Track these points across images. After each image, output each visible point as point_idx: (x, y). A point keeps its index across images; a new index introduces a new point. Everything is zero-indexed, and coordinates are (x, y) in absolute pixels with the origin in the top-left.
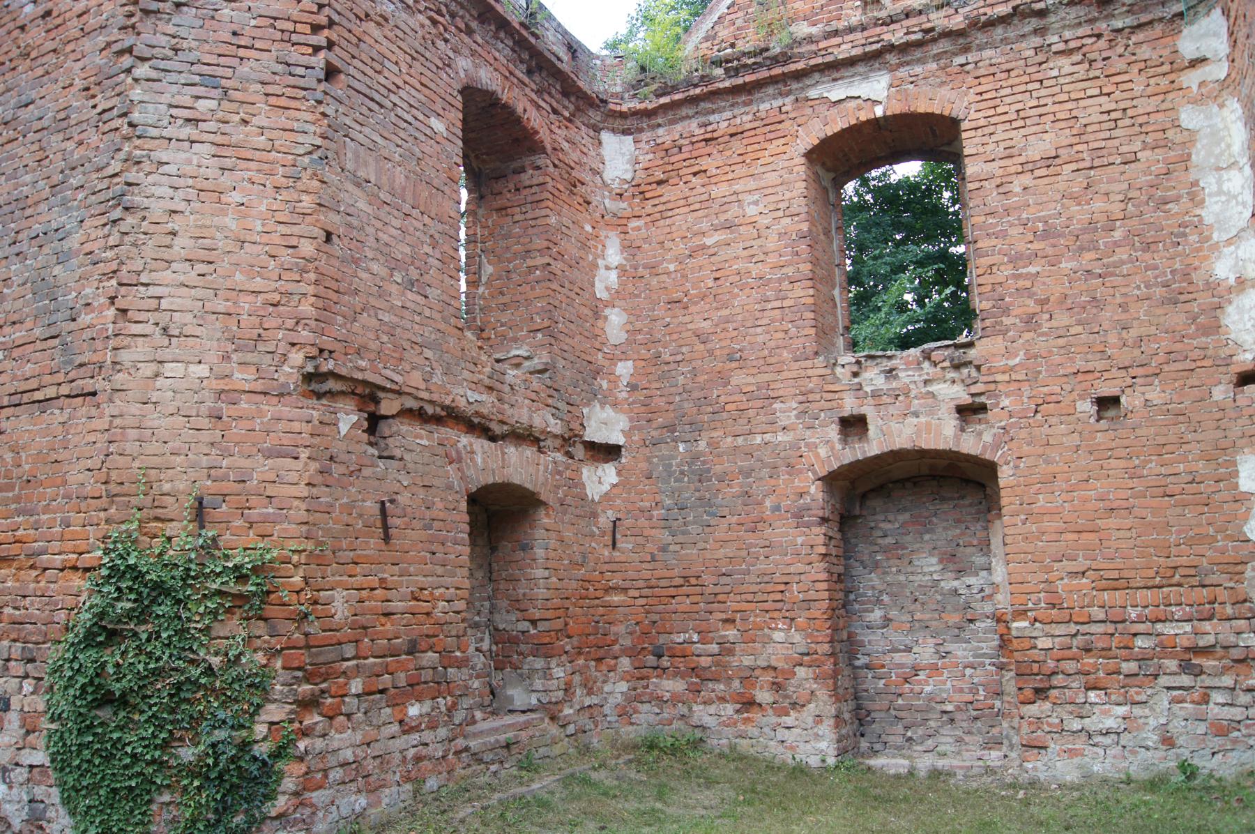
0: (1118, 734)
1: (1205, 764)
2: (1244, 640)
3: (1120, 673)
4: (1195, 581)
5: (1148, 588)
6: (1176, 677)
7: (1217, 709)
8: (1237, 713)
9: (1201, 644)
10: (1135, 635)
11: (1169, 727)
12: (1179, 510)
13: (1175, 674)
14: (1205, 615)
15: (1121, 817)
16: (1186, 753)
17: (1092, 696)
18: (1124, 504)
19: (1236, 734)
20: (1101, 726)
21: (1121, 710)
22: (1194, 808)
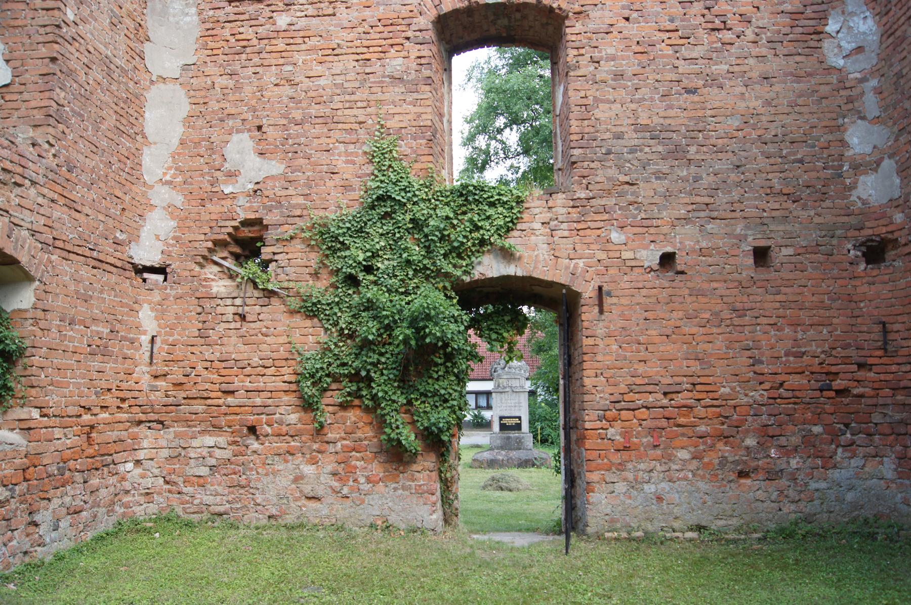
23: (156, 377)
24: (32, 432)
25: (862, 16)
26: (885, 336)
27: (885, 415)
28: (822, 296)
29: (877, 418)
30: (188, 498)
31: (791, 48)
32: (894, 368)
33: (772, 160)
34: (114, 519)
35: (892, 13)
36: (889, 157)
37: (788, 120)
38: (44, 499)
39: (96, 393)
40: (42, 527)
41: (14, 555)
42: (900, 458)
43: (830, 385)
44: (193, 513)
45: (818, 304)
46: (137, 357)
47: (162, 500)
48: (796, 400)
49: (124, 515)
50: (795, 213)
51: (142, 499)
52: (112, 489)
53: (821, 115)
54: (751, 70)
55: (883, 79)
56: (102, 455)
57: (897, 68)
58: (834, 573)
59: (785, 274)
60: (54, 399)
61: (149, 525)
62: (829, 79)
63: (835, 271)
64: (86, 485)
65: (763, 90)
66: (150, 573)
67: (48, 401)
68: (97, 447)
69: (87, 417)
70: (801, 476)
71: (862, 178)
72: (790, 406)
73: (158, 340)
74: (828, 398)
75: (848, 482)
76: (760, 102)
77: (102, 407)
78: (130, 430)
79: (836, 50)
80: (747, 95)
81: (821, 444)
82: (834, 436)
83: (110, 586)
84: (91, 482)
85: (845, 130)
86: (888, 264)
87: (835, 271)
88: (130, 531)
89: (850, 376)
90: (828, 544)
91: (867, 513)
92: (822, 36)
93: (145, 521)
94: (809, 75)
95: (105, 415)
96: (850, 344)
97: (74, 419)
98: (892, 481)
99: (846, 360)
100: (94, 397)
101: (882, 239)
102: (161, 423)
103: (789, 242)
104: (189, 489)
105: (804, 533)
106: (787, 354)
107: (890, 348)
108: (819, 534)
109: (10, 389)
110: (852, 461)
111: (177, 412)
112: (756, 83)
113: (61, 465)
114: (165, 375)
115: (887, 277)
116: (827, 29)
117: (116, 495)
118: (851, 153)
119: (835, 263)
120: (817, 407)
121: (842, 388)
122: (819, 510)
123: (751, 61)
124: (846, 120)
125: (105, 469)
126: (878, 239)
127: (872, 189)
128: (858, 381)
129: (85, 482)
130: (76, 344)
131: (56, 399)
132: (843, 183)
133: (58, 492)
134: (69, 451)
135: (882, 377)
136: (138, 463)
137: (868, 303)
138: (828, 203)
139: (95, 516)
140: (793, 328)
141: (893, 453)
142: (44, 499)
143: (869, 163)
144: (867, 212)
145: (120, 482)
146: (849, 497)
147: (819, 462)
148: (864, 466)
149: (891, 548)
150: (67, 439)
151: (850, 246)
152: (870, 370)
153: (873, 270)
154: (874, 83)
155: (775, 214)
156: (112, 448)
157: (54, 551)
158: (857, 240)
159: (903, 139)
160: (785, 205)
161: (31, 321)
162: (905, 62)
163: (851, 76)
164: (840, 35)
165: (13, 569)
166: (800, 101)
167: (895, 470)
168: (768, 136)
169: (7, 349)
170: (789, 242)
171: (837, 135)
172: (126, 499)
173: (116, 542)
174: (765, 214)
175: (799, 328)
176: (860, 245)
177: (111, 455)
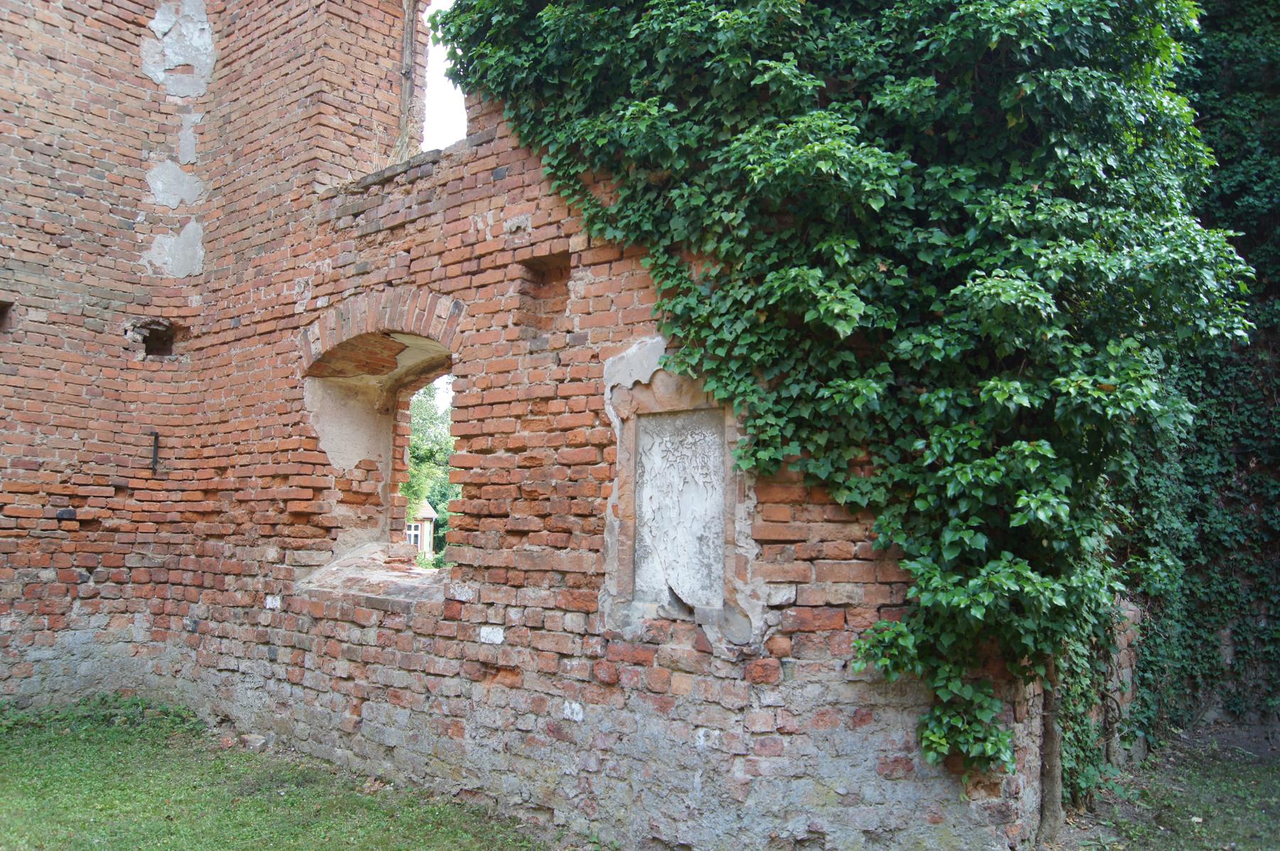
25: (200, 26)
26: (156, 453)
27: (143, 556)
28: (79, 388)
29: (132, 560)
31: (96, 30)
32: (162, 495)
33: (37, 179)
35: (233, 38)
36: (197, 220)
37: (73, 129)
42: (155, 614)
43: (75, 513)
45: (73, 398)
48: (20, 531)
50: (58, 264)
53: (121, 137)
54: (31, 38)
55: (208, 116)
57: (225, 110)
58: (40, 776)
59: (28, 347)
62: (140, 91)
63: (103, 356)
65: (44, 74)
70: (15, 642)
71: (159, 238)
72: (10, 540)
74: (69, 531)
75: (84, 648)
76: (34, 89)
79: (158, 58)
80: (17, 71)
81: (50, 595)
82: (70, 584)
85: (148, 168)
86: (173, 358)
87: (103, 356)
89: (103, 502)
90: (44, 737)
91: (107, 689)
92: (142, 30)
94: (114, 76)
96: (108, 458)
98: (143, 644)
99: (101, 480)
101: (171, 324)
103: (42, 302)
105: (10, 723)
106: (14, 465)
107: (160, 469)
108: (32, 724)
110: (93, 619)
112: (34, 59)
115: (170, 374)
116: (152, 24)
118: (148, 200)
119: (103, 345)
120: (51, 543)
121: (90, 517)
122: (38, 689)
123: (34, 26)
124: (152, 155)
126: (166, 323)
127: (172, 256)
128: (113, 510)
132: (133, 239)
135: (146, 506)
137: (140, 405)
138: (107, 260)
140: (29, 426)
141: (148, 606)
143: (170, 221)
144: (156, 284)
146: (84, 668)
147: (45, 621)
148: (108, 625)
149: (130, 734)
151: (128, 325)
152: (132, 495)
153: (153, 362)
154: (196, 117)
155: (27, 257)
158: (139, 319)
159: (218, 201)
160: (44, 248)
162: (236, 106)
163: (169, 99)
164: (166, 38)
166: (95, 108)
167: (149, 629)
168: (38, 143)
170: (42, 302)
171: (137, 172)
174: (12, 255)
175: (38, 429)
176: (141, 327)
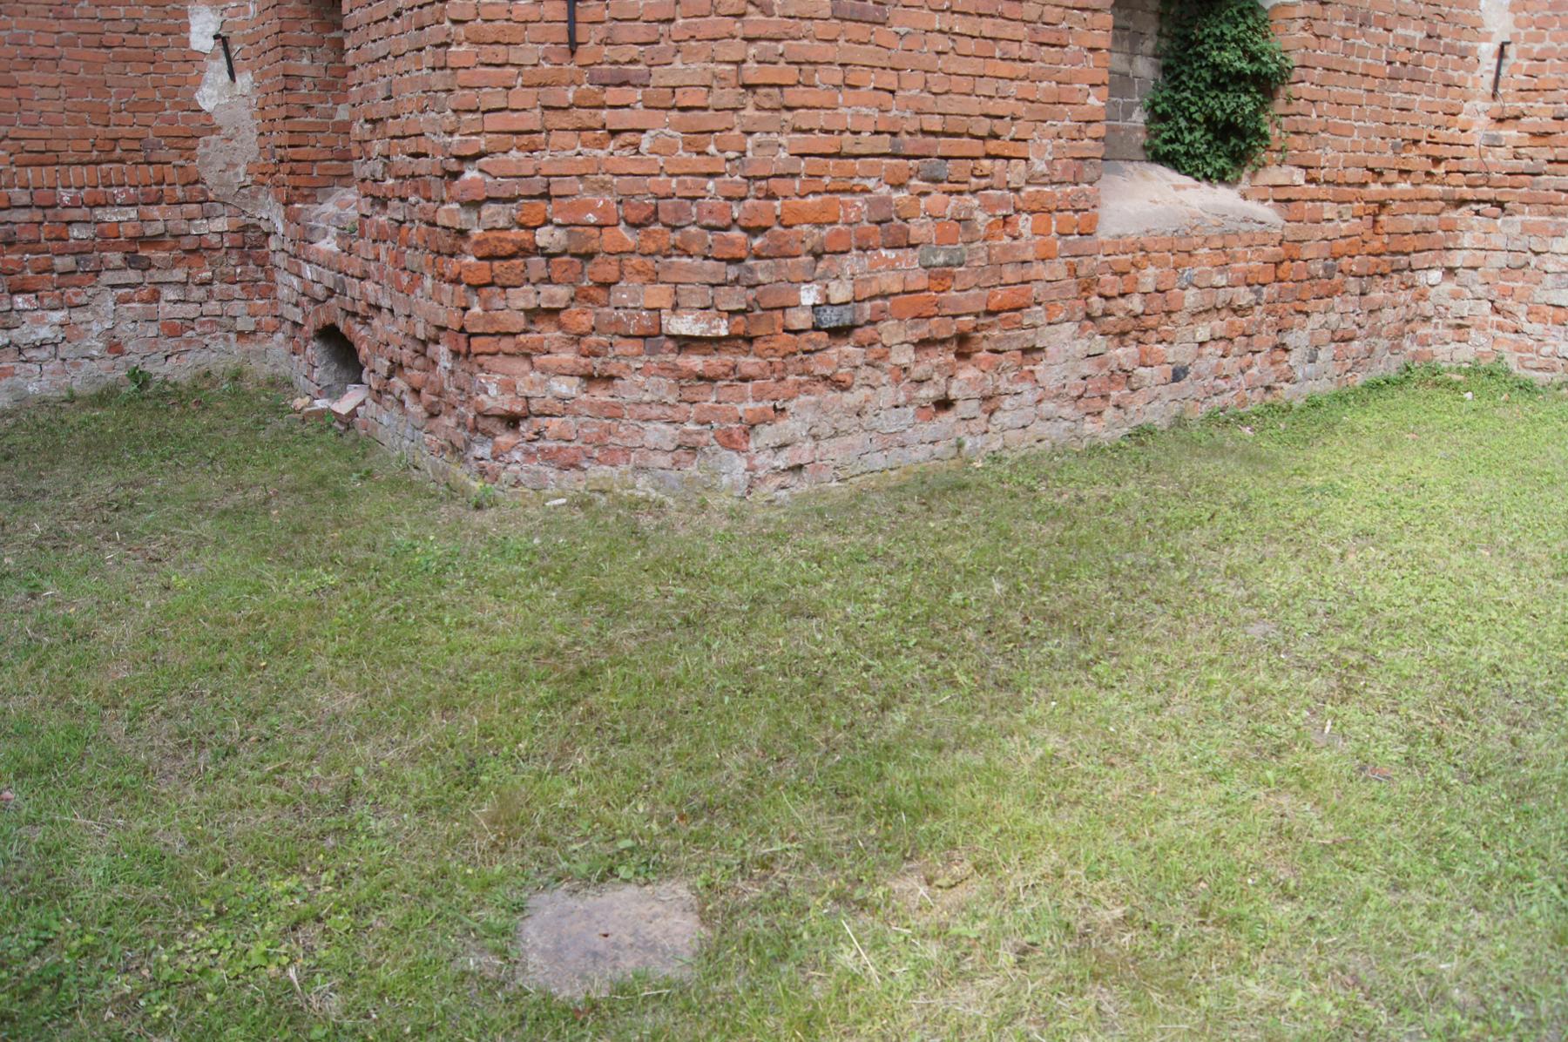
0: (56, 345)
1: (158, 369)
2: (196, 227)
3: (52, 271)
4: (139, 157)
5: (83, 164)
6: (121, 273)
7: (168, 307)
8: (190, 310)
9: (149, 232)
10: (69, 223)
11: (117, 332)
12: (119, 66)
13: (120, 269)
14: (153, 198)
15: (70, 436)
16: (137, 360)
17: (20, 301)
18: (49, 53)
19: (190, 333)
20: (33, 337)
21: (57, 316)
22: (151, 417)
23: (1500, 120)
24: (1292, 205)
30: (1530, 342)
34: (1399, 360)
38: (1300, 312)
39: (1393, 147)
40: (1293, 354)
41: (1252, 389)
44: (1537, 369)
46: (1469, 84)
47: (1483, 340)
49: (1415, 356)
51: (1450, 334)
52: (1402, 311)
56: (1393, 253)
60: (1327, 155)
61: (1456, 377)
64: (1364, 298)
66: (1453, 449)
67: (1319, 158)
68: (1386, 239)
69: (1376, 188)
73: (1511, 51)
77: (1401, 172)
78: (1444, 215)
83: (1389, 456)
84: (1372, 295)
88: (1423, 382)
93: (1450, 369)
95: (1404, 186)
97: (1355, 189)
100: (1390, 153)
102: (1500, 205)
104: (1537, 328)
109: (1264, 136)
111: (1532, 186)
113: (1330, 262)
114: (1517, 118)
117: (1408, 322)
125: (1396, 276)
129: (1363, 294)
130: (1369, 61)
131: (1331, 153)
133: (1322, 304)
134: (1342, 241)
136: (1450, 271)
139: (1372, 350)
142: (1300, 312)
145: (1417, 301)
150: (1342, 221)
156: (1411, 243)
157: (1306, 393)
161: (1301, 22)
165: (1249, 408)
169: (1264, 70)
172: (1423, 330)
173: (1400, 397)
177: (1408, 254)
